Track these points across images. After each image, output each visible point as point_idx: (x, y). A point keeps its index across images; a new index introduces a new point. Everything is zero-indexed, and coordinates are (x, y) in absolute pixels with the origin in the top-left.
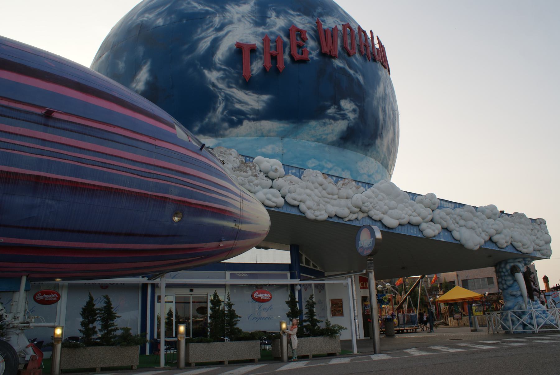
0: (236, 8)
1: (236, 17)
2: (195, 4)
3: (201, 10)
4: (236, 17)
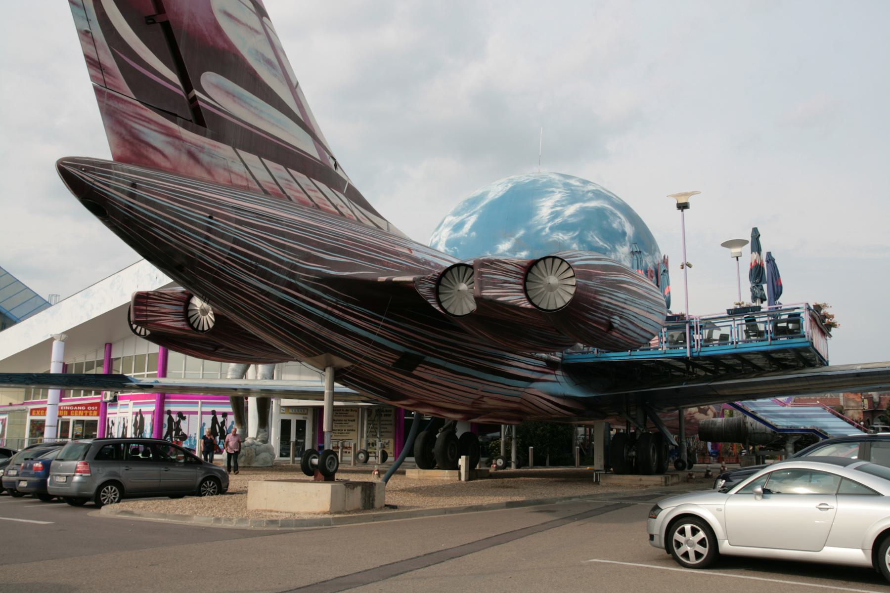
0: (621, 247)
1: (623, 256)
2: (597, 239)
3: (602, 245)
4: (623, 256)
